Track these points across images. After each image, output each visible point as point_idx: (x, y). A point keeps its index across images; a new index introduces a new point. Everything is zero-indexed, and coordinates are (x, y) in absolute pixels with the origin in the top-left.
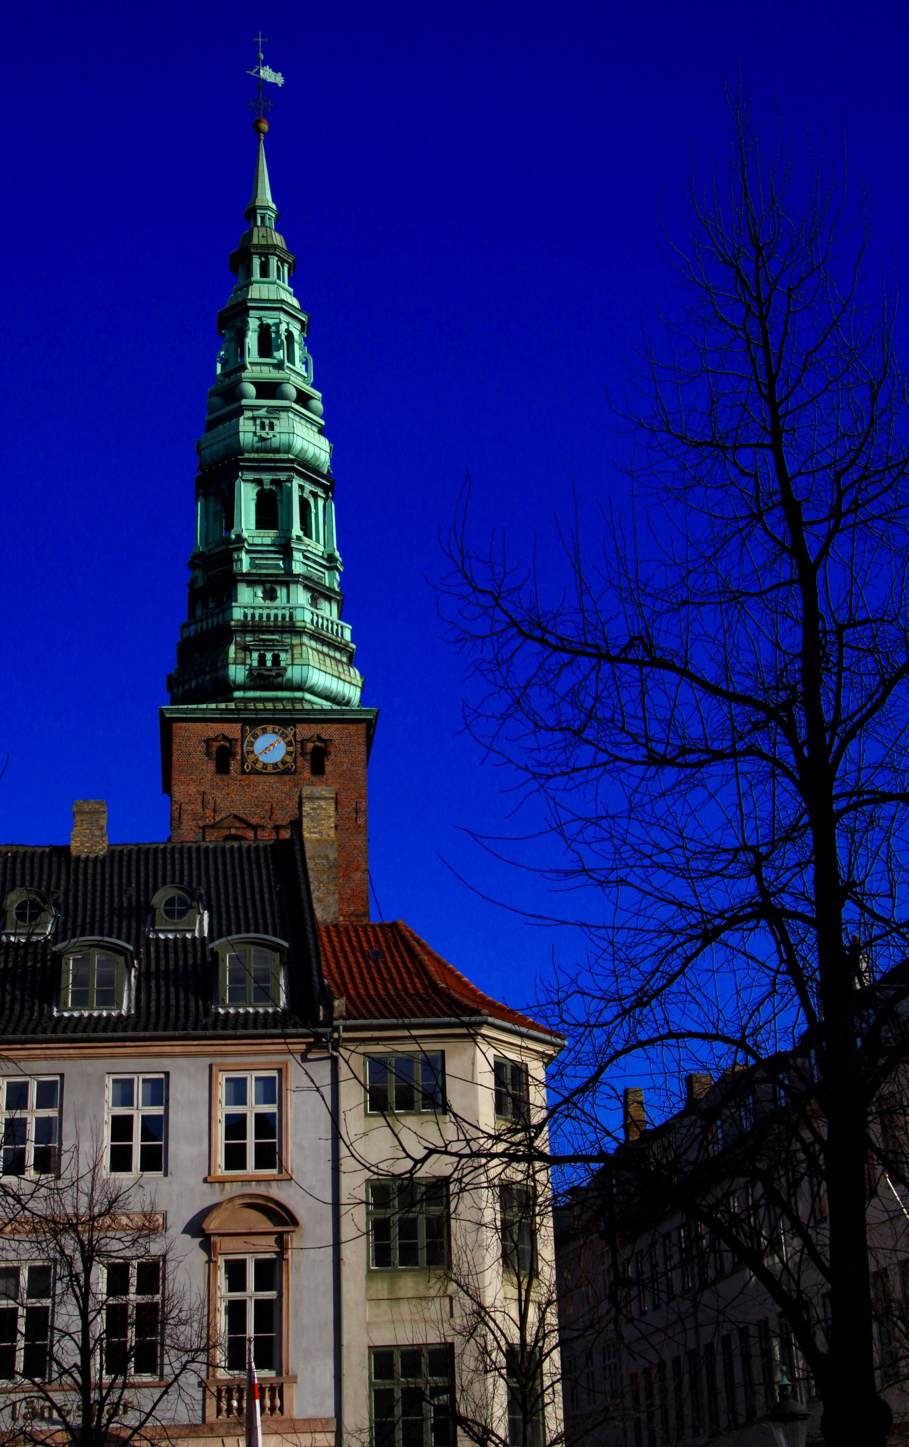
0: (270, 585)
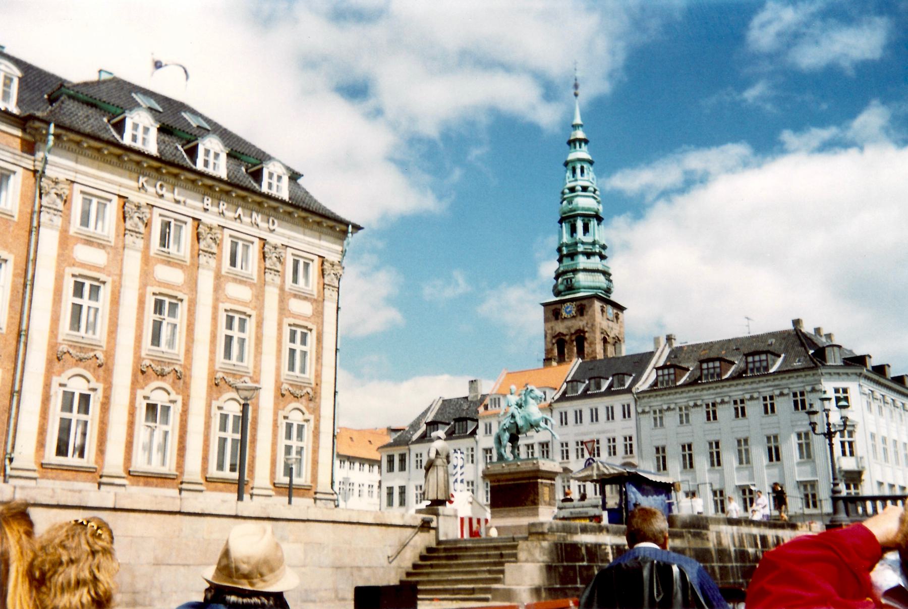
0: (588, 255)
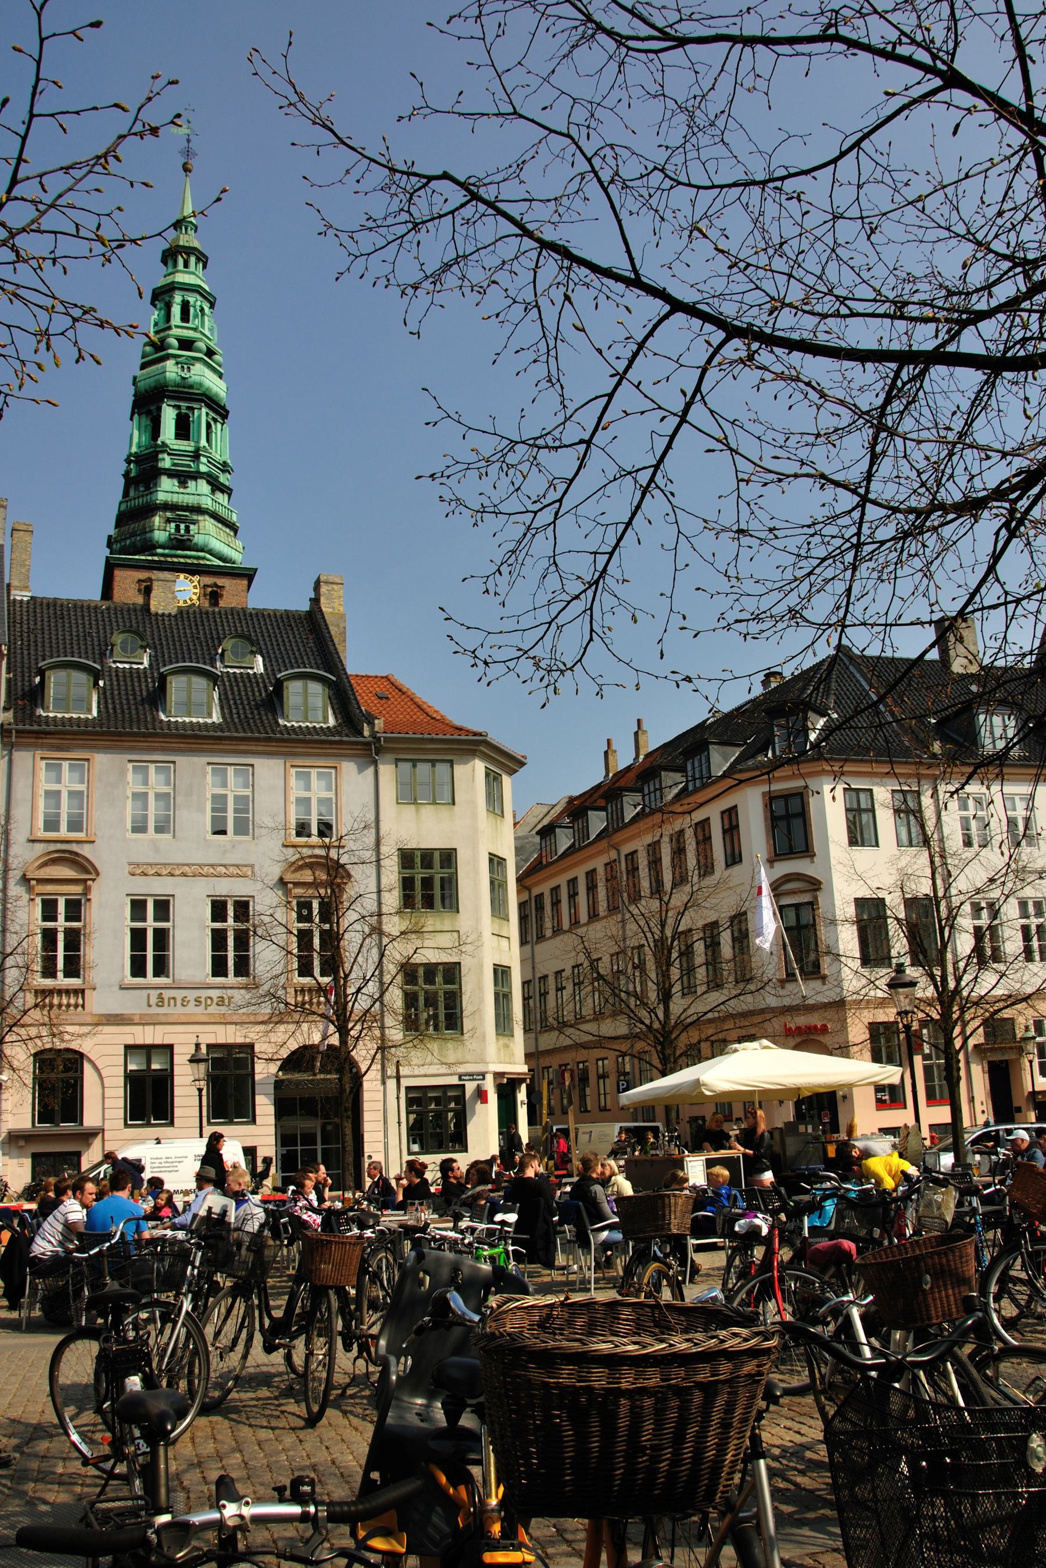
0: (183, 477)
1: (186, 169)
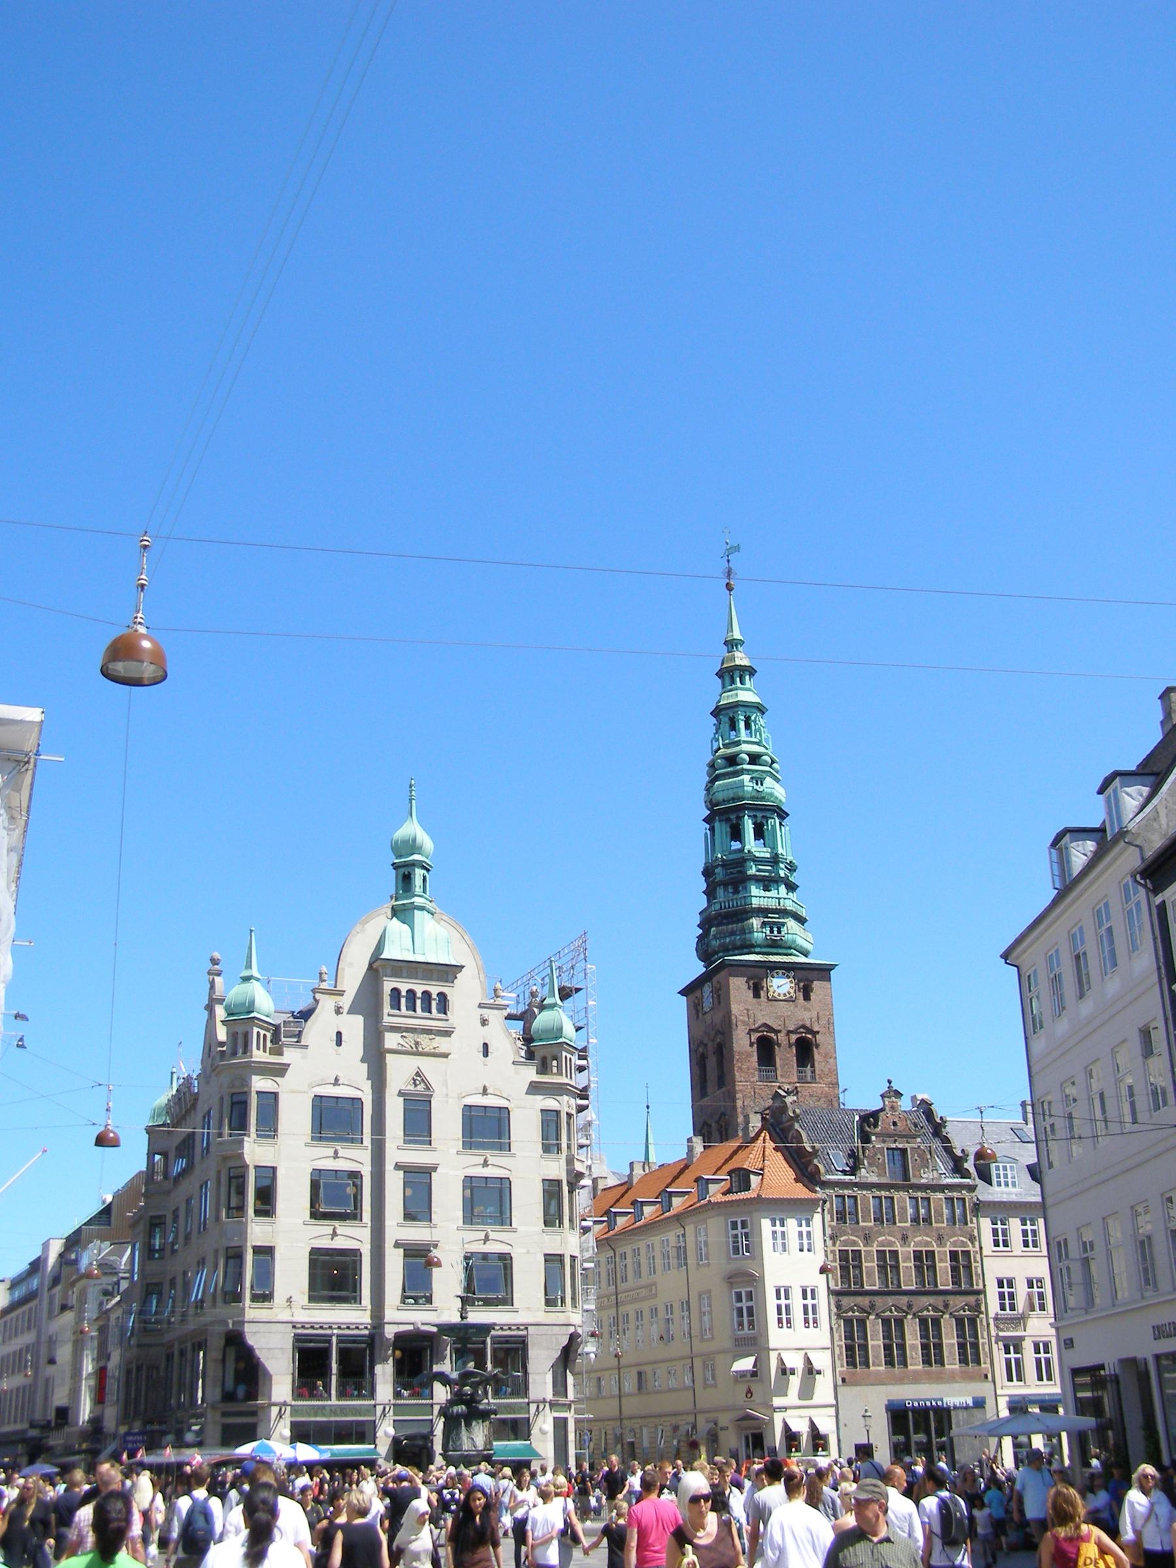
0: (767, 883)
1: (729, 587)
